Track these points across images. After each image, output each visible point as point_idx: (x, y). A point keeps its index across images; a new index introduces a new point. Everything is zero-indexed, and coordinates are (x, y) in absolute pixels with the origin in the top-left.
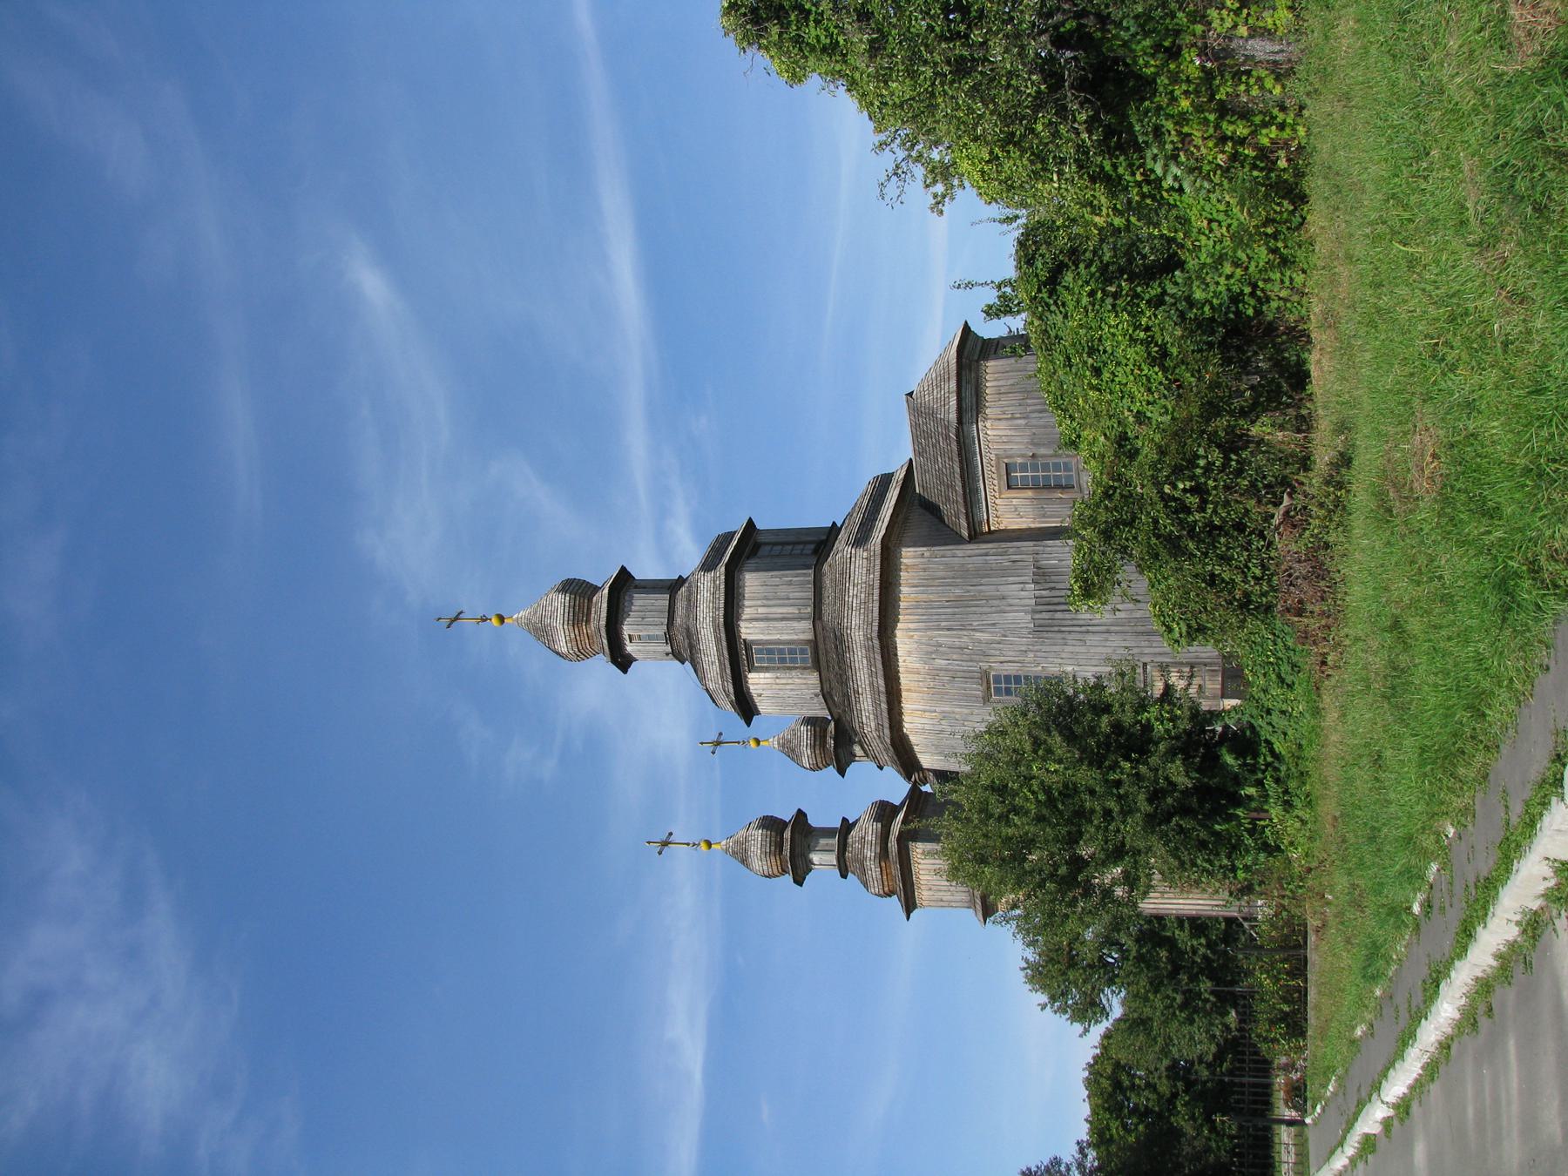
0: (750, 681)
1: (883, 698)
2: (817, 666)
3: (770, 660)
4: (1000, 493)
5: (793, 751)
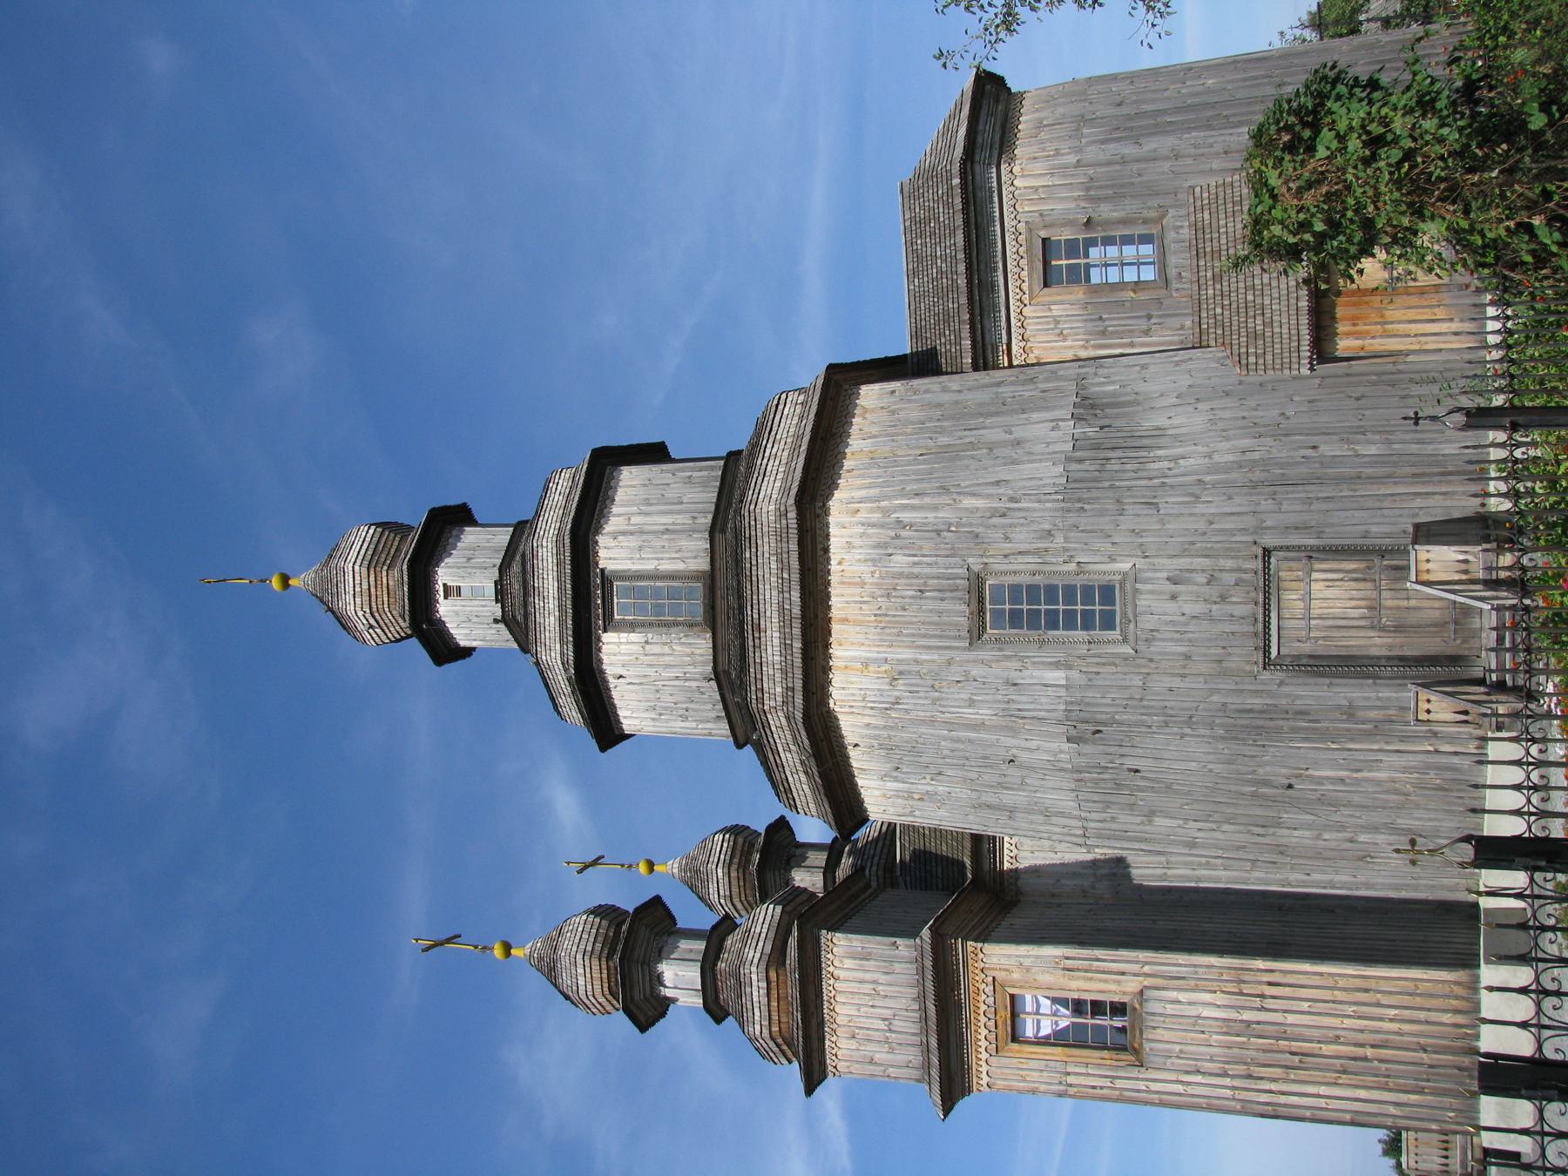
1: (797, 631)
2: (711, 621)
3: (641, 609)
4: (1031, 299)
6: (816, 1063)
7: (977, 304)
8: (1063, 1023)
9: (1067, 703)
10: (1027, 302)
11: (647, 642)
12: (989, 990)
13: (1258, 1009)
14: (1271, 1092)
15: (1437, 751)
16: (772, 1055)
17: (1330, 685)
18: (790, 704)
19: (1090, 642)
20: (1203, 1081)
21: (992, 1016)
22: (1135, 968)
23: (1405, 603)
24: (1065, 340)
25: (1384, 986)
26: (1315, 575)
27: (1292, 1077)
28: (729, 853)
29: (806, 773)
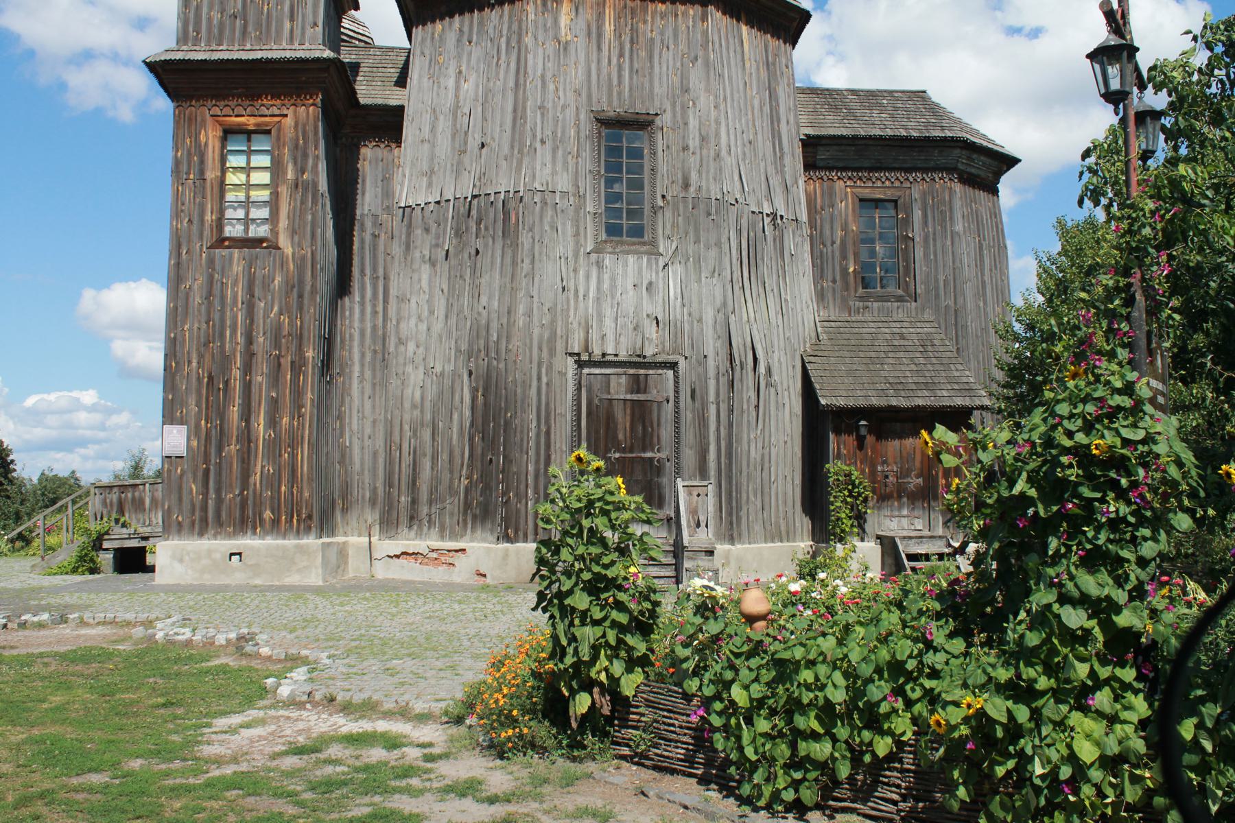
19: (595, 214)
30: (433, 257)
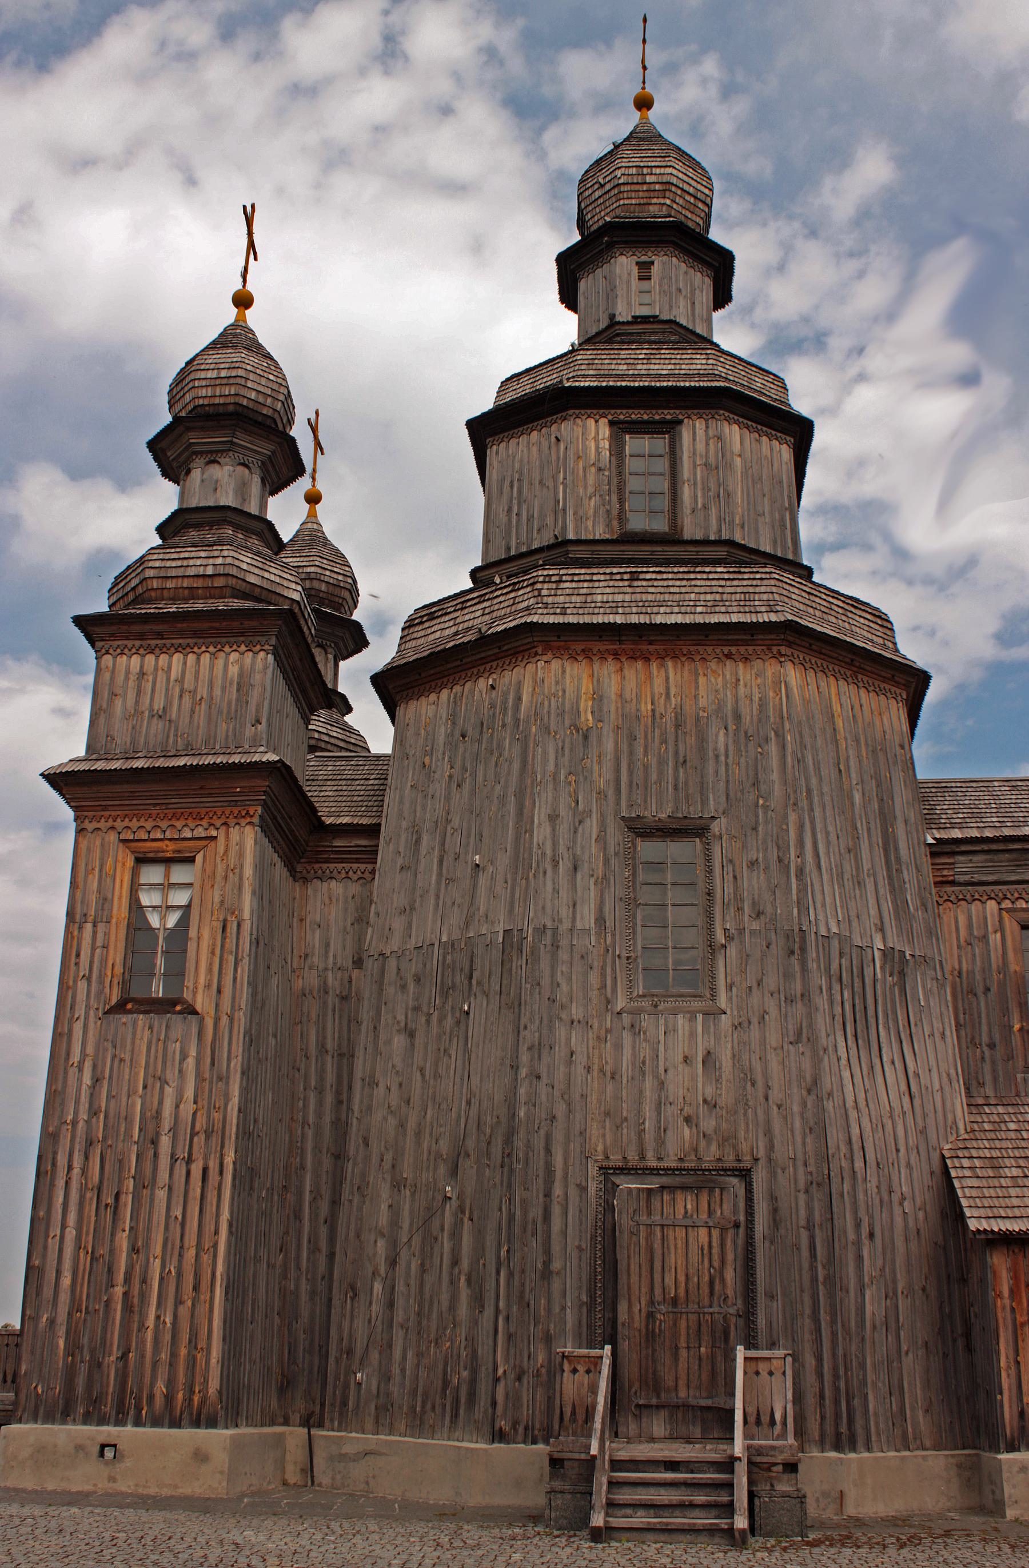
0: (591, 422)
1: (634, 619)
4: (1008, 910)
5: (311, 546)
6: (113, 629)
7: (1001, 847)
8: (154, 920)
9: (555, 930)
10: (1003, 906)
11: (600, 469)
12: (200, 832)
13: (173, 1155)
14: (70, 1168)
15: (497, 1380)
16: (122, 584)
17: (580, 1249)
18: (545, 611)
19: (628, 958)
20: (84, 1087)
21: (168, 835)
22: (226, 1005)
23: (683, 1343)
24: (959, 947)
25: (202, 1309)
26: (716, 1233)
27: (89, 1195)
28: (331, 581)
29: (456, 634)
30: (409, 1025)
